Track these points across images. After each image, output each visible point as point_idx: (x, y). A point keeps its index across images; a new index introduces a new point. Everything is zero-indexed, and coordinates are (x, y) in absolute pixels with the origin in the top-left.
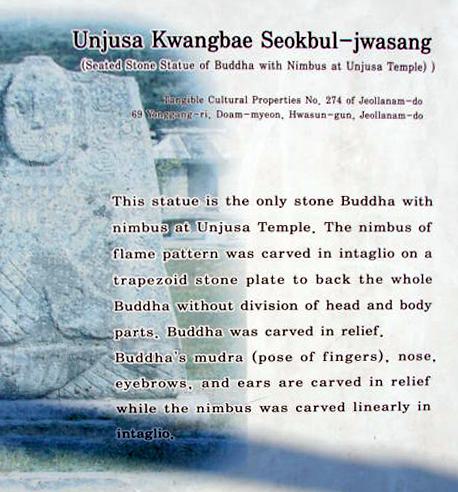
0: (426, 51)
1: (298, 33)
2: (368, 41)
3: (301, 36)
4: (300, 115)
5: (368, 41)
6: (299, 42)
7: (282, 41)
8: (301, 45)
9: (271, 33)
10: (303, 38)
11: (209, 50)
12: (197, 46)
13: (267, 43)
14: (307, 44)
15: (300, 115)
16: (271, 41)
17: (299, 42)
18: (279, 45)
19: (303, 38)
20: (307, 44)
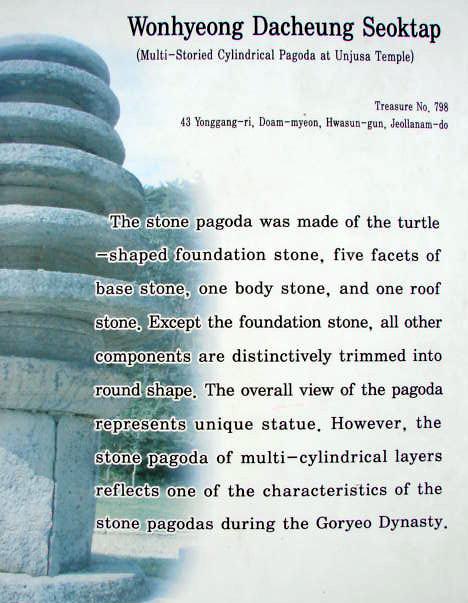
0: (237, 37)
1: (400, 19)
2: (138, 22)
3: (402, 23)
4: (336, 124)
5: (138, 22)
6: (401, 30)
7: (384, 29)
8: (403, 33)
9: (372, 19)
10: (406, 25)
11: (233, 38)
12: (332, 34)
13: (369, 31)
14: (409, 32)
15: (336, 124)
16: (375, 29)
17: (401, 30)
18: (381, 33)
19: (406, 25)
20: (409, 32)
